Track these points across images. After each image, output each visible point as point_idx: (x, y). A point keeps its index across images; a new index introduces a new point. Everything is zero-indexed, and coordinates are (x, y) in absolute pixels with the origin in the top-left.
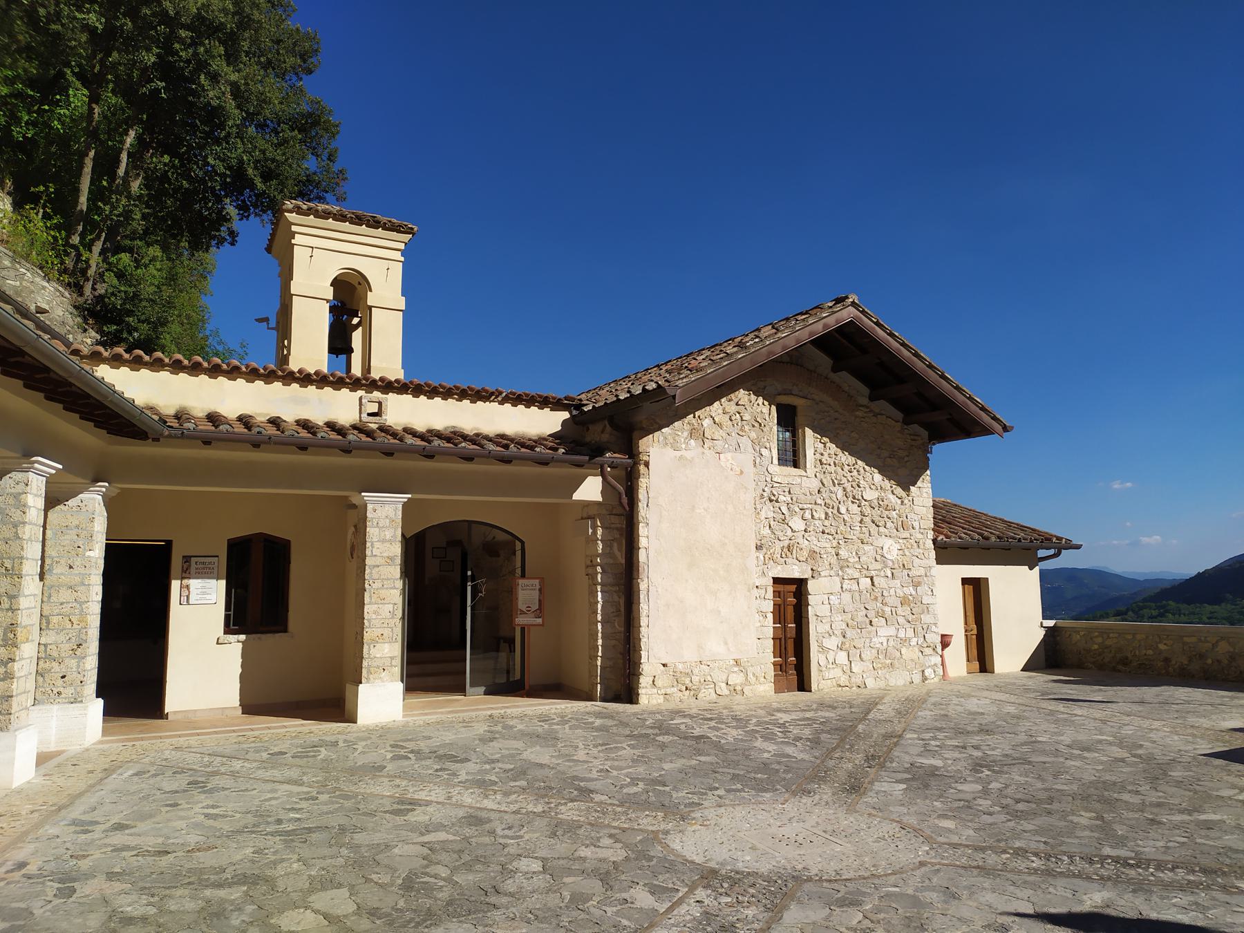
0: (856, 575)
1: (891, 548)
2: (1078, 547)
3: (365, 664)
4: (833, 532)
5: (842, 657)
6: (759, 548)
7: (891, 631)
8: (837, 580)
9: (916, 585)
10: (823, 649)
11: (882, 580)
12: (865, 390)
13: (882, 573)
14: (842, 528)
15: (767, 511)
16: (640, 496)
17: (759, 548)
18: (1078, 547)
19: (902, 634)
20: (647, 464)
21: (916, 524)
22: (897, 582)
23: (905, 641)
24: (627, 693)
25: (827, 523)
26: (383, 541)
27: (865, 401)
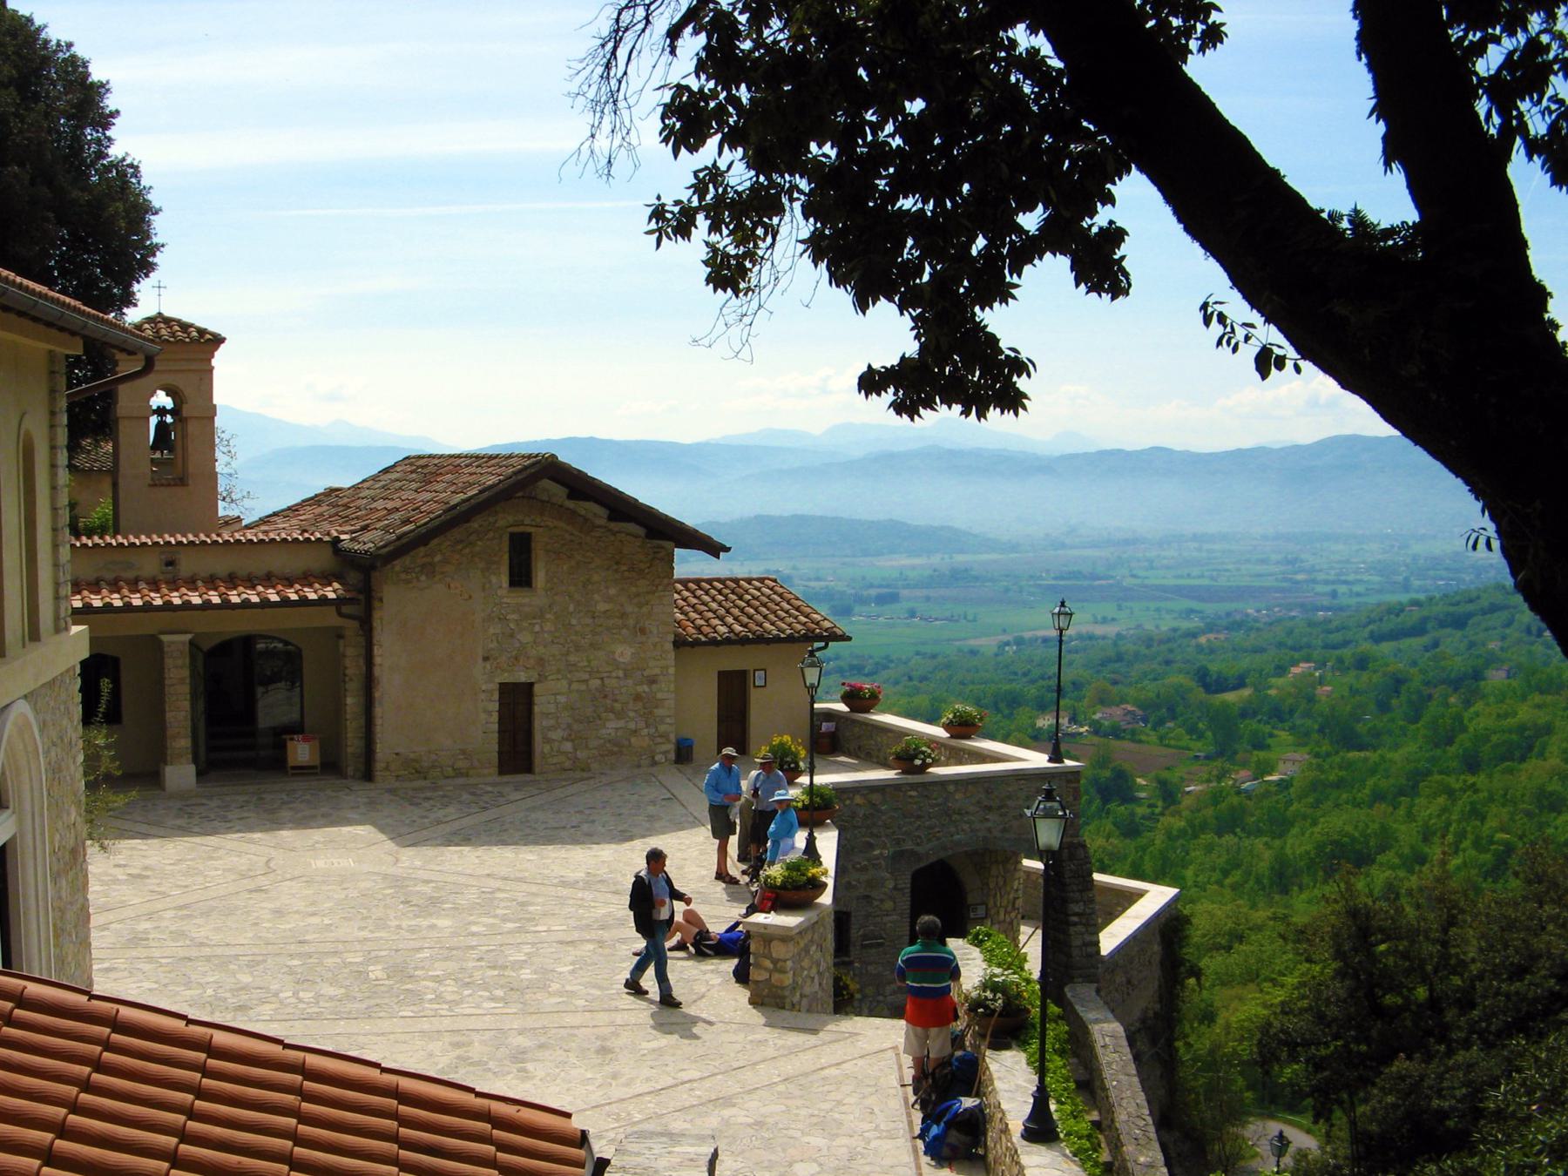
0: (586, 676)
1: (624, 653)
2: (849, 639)
3: (169, 752)
4: (562, 641)
5: (568, 746)
6: (486, 659)
7: (621, 724)
8: (565, 683)
9: (652, 681)
10: (548, 741)
11: (614, 681)
12: (602, 512)
13: (614, 674)
14: (574, 638)
15: (494, 629)
16: (375, 624)
17: (486, 659)
18: (849, 639)
19: (632, 726)
20: (381, 600)
21: (655, 631)
22: (630, 682)
23: (635, 732)
24: (368, 775)
25: (557, 634)
26: (176, 667)
27: (603, 522)
